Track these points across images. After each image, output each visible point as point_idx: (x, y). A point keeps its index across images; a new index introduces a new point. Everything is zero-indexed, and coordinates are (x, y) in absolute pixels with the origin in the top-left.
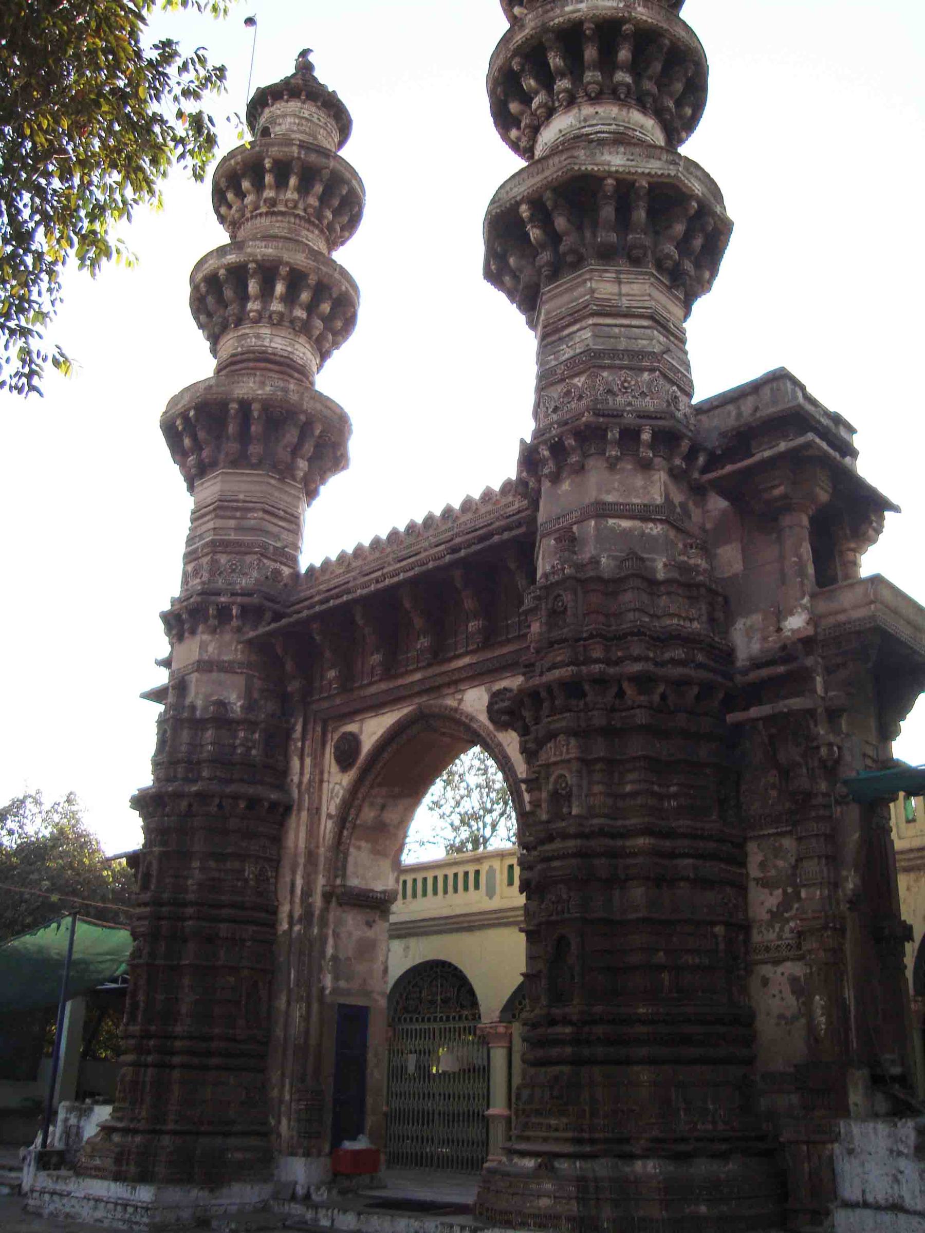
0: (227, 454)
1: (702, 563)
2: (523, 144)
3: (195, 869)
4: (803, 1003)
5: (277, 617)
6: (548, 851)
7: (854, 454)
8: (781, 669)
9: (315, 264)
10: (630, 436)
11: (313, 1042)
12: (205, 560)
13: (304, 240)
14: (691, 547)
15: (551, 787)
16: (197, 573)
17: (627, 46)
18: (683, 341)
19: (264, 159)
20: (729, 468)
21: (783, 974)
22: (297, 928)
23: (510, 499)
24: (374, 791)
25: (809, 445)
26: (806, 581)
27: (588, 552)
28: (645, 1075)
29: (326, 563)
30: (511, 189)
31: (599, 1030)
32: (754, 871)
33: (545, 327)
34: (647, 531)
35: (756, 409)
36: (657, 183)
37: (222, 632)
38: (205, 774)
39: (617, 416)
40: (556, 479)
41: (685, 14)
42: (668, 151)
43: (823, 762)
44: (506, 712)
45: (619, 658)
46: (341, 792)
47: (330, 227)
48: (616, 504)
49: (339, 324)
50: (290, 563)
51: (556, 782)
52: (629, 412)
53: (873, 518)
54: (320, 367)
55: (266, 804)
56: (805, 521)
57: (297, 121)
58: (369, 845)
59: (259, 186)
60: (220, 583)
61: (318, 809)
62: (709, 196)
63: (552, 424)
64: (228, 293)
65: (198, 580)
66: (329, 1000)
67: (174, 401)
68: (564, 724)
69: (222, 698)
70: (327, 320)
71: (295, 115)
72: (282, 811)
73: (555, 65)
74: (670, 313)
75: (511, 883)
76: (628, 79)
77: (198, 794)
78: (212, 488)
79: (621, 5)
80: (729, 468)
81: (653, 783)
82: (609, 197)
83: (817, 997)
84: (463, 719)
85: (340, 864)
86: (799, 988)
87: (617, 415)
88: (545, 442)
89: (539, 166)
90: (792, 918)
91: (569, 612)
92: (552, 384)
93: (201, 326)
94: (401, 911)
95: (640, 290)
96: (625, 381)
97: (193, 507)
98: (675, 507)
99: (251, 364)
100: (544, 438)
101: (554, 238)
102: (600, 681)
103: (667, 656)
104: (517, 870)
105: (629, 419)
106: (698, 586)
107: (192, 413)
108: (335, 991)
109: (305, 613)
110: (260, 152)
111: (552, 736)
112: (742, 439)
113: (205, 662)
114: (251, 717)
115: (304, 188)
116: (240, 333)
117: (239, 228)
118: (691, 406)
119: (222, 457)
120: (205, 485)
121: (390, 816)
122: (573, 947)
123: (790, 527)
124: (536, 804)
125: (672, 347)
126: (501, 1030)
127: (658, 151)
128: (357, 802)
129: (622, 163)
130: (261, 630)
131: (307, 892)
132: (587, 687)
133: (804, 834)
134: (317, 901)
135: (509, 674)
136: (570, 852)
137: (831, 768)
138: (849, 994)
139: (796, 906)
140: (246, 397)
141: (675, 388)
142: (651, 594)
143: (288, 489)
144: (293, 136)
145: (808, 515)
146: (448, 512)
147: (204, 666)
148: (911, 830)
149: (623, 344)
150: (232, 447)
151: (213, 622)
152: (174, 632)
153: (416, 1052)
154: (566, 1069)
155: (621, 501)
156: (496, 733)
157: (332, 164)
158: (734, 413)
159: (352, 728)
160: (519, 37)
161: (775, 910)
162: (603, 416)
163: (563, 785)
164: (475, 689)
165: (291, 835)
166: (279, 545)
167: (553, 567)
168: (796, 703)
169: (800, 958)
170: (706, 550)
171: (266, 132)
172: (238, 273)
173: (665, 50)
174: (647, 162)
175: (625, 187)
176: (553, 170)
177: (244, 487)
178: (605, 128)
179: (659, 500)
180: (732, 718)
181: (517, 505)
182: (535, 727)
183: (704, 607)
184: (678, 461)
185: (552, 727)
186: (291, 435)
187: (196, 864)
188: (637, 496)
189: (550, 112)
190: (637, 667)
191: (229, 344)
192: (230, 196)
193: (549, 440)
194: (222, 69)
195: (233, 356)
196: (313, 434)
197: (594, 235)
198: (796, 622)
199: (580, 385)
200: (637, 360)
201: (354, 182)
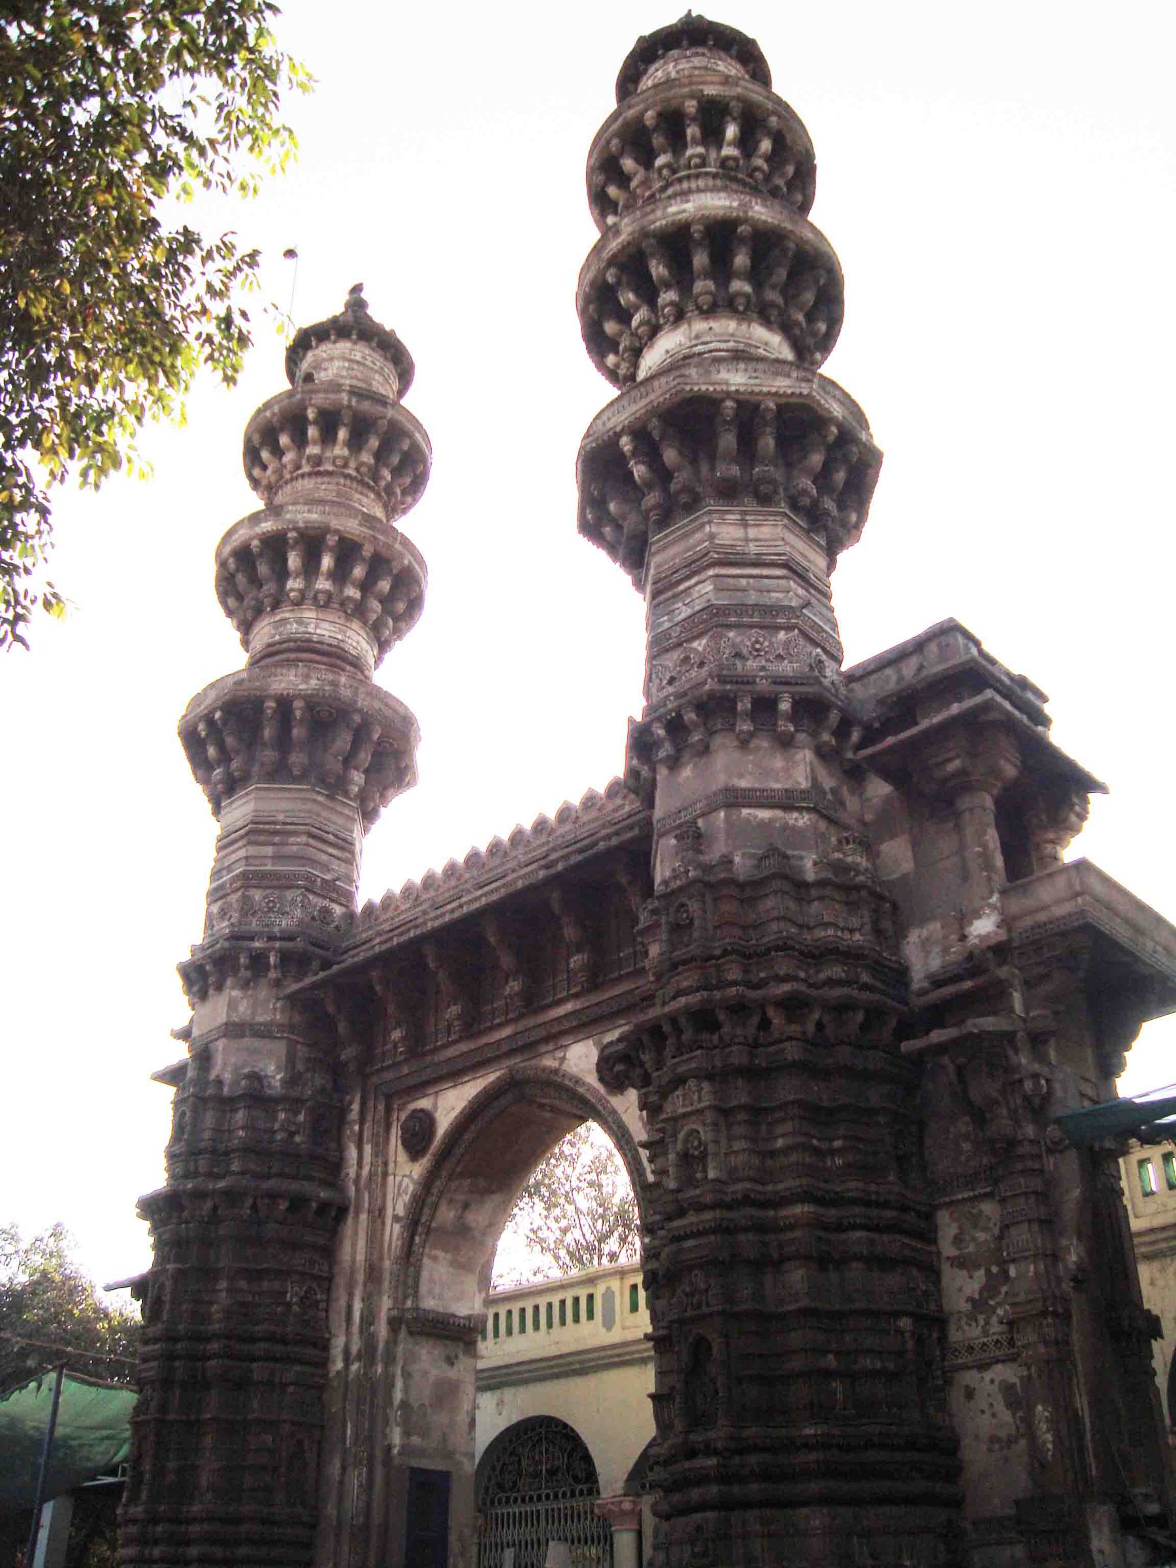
0: (262, 765)
1: (862, 861)
2: (622, 371)
3: (220, 1290)
4: (1022, 1419)
5: (326, 965)
6: (678, 1228)
7: (1045, 721)
8: (968, 984)
9: (371, 532)
10: (765, 706)
11: (377, 1518)
12: (234, 898)
13: (356, 505)
14: (848, 843)
15: (679, 1146)
16: (225, 914)
17: (744, 250)
18: (828, 597)
19: (305, 409)
20: (890, 740)
21: (992, 1381)
22: (354, 1367)
23: (618, 801)
24: (453, 1186)
25: (988, 706)
26: (995, 877)
27: (717, 851)
28: (815, 1519)
29: (388, 900)
30: (609, 419)
31: (753, 1459)
32: (947, 1249)
33: (655, 583)
34: (791, 822)
35: (921, 667)
36: (787, 404)
37: (255, 988)
38: (235, 1167)
39: (748, 683)
40: (674, 763)
41: (814, 216)
42: (798, 367)
43: (1026, 1098)
44: (617, 1070)
45: (762, 980)
46: (411, 1188)
47: (389, 490)
48: (754, 790)
49: (401, 607)
50: (343, 900)
51: (686, 1141)
52: (762, 678)
53: (1075, 800)
54: (378, 660)
55: (314, 1205)
56: (989, 802)
57: (347, 364)
58: (449, 1256)
59: (301, 441)
60: (254, 925)
61: (382, 1210)
62: (850, 418)
63: (666, 697)
64: (263, 569)
65: (226, 923)
66: (397, 1462)
67: (197, 700)
68: (694, 1065)
69: (256, 1070)
70: (387, 601)
71: (345, 359)
72: (335, 1214)
73: (658, 274)
74: (809, 561)
75: (634, 1308)
76: (748, 289)
77: (227, 1193)
78: (241, 809)
79: (735, 204)
80: (890, 740)
81: (813, 1137)
82: (729, 423)
83: (1040, 1408)
84: (567, 1082)
85: (410, 1281)
86: (1014, 1399)
87: (747, 681)
88: (659, 719)
89: (642, 389)
90: (999, 1304)
91: (696, 922)
92: (667, 651)
93: (230, 613)
94: (494, 1351)
95: (771, 533)
96: (757, 642)
97: (219, 832)
98: (825, 793)
99: (293, 656)
100: (657, 714)
101: (663, 475)
102: (739, 1009)
103: (822, 976)
104: (642, 1294)
105: (763, 686)
106: (858, 888)
107: (218, 715)
108: (406, 1449)
109: (362, 957)
110: (303, 400)
111: (679, 1081)
112: (905, 705)
113: (235, 1024)
114: (295, 1093)
115: (356, 442)
116: (278, 618)
117: (276, 493)
118: (840, 674)
119: (256, 769)
120: (234, 806)
121: (477, 1218)
122: (715, 1351)
123: (971, 810)
124: (660, 1173)
125: (813, 600)
126: (627, 1506)
127: (787, 368)
128: (431, 1200)
129: (742, 381)
130: (309, 980)
131: (368, 1319)
132: (722, 1017)
133: (1008, 1194)
134: (382, 1330)
135: (623, 1022)
136: (707, 1226)
137: (1039, 1107)
138: (1082, 1403)
139: (1004, 1289)
141: (819, 650)
142: (799, 900)
143: (339, 808)
144: (342, 381)
145: (992, 796)
146: (541, 826)
147: (234, 1030)
148: (1151, 1206)
149: (752, 598)
150: (269, 755)
151: (244, 974)
152: (195, 988)
153: (514, 1545)
154: (711, 1515)
155: (757, 785)
156: (610, 1098)
157: (390, 413)
158: (894, 678)
159: (424, 1103)
160: (614, 244)
161: (977, 1296)
162: (731, 682)
163: (696, 1143)
164: (580, 1044)
165: (347, 1247)
166: (328, 877)
167: (674, 870)
168: (988, 1023)
169: (1012, 1359)
170: (868, 847)
171: (309, 378)
172: (275, 545)
173: (790, 254)
174: (774, 379)
175: (748, 411)
176: (658, 394)
177: (284, 805)
178: (723, 346)
179: (804, 784)
180: (906, 1046)
181: (627, 809)
182: (658, 1073)
183: (866, 913)
184: (826, 737)
185: (680, 1070)
186: (343, 741)
187: (223, 1284)
188: (777, 781)
189: (654, 331)
190: (786, 987)
191: (264, 632)
192: (265, 455)
194: (254, 255)
195: (270, 645)
196: (370, 739)
197: (713, 468)
198: (984, 927)
199: (700, 649)
200: (769, 617)
201: (417, 435)
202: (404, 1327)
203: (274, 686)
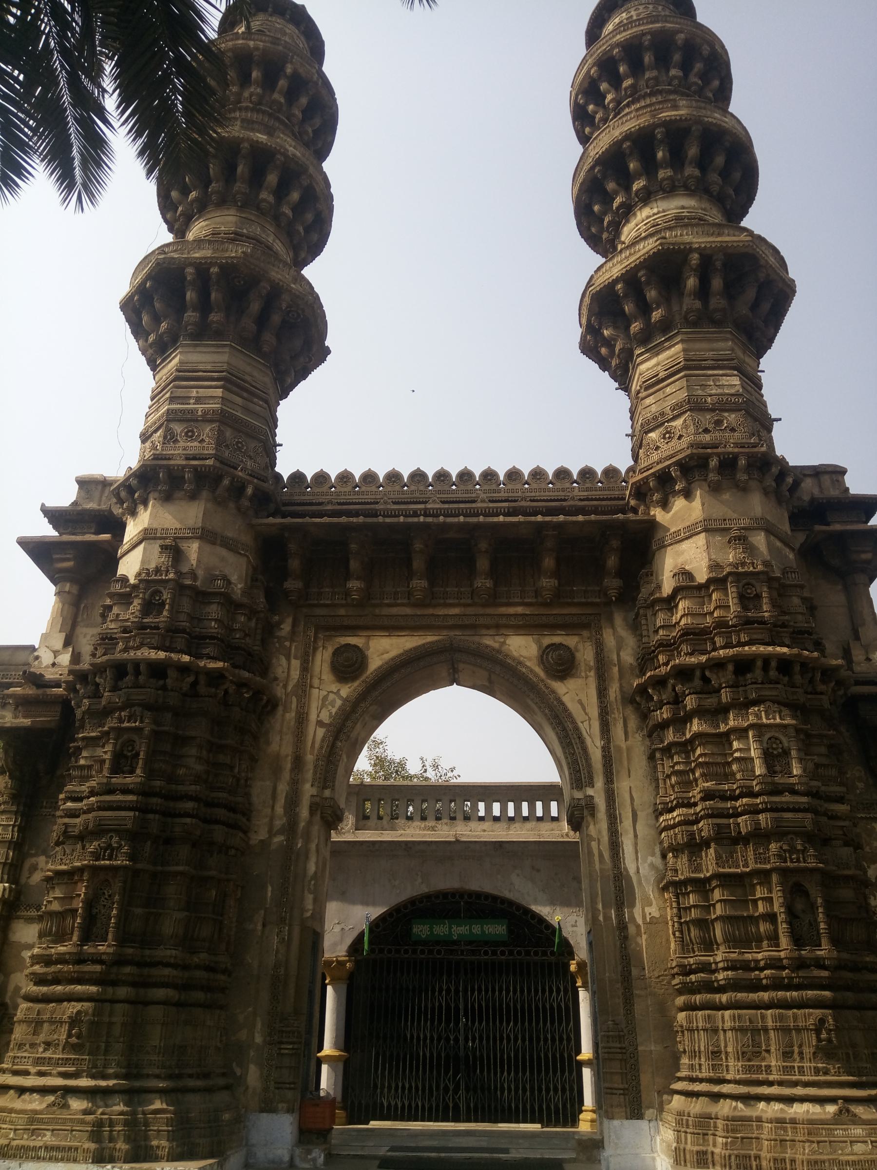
120: (198, 349)
131: (293, 802)
134: (304, 813)
150: (248, 324)
193: (724, 453)
202: (319, 812)
203: (273, 273)
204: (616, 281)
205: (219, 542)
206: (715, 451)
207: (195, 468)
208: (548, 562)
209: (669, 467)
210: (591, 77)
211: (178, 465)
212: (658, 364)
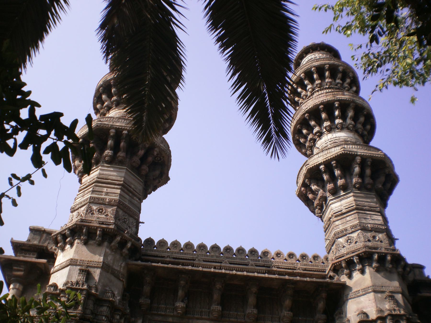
107: (125, 132)
140: (156, 143)
150: (136, 160)
204: (320, 164)
205: (110, 271)
206: (376, 251)
207: (103, 229)
208: (288, 302)
209: (353, 257)
210: (300, 77)
211: (94, 226)
212: (341, 205)
